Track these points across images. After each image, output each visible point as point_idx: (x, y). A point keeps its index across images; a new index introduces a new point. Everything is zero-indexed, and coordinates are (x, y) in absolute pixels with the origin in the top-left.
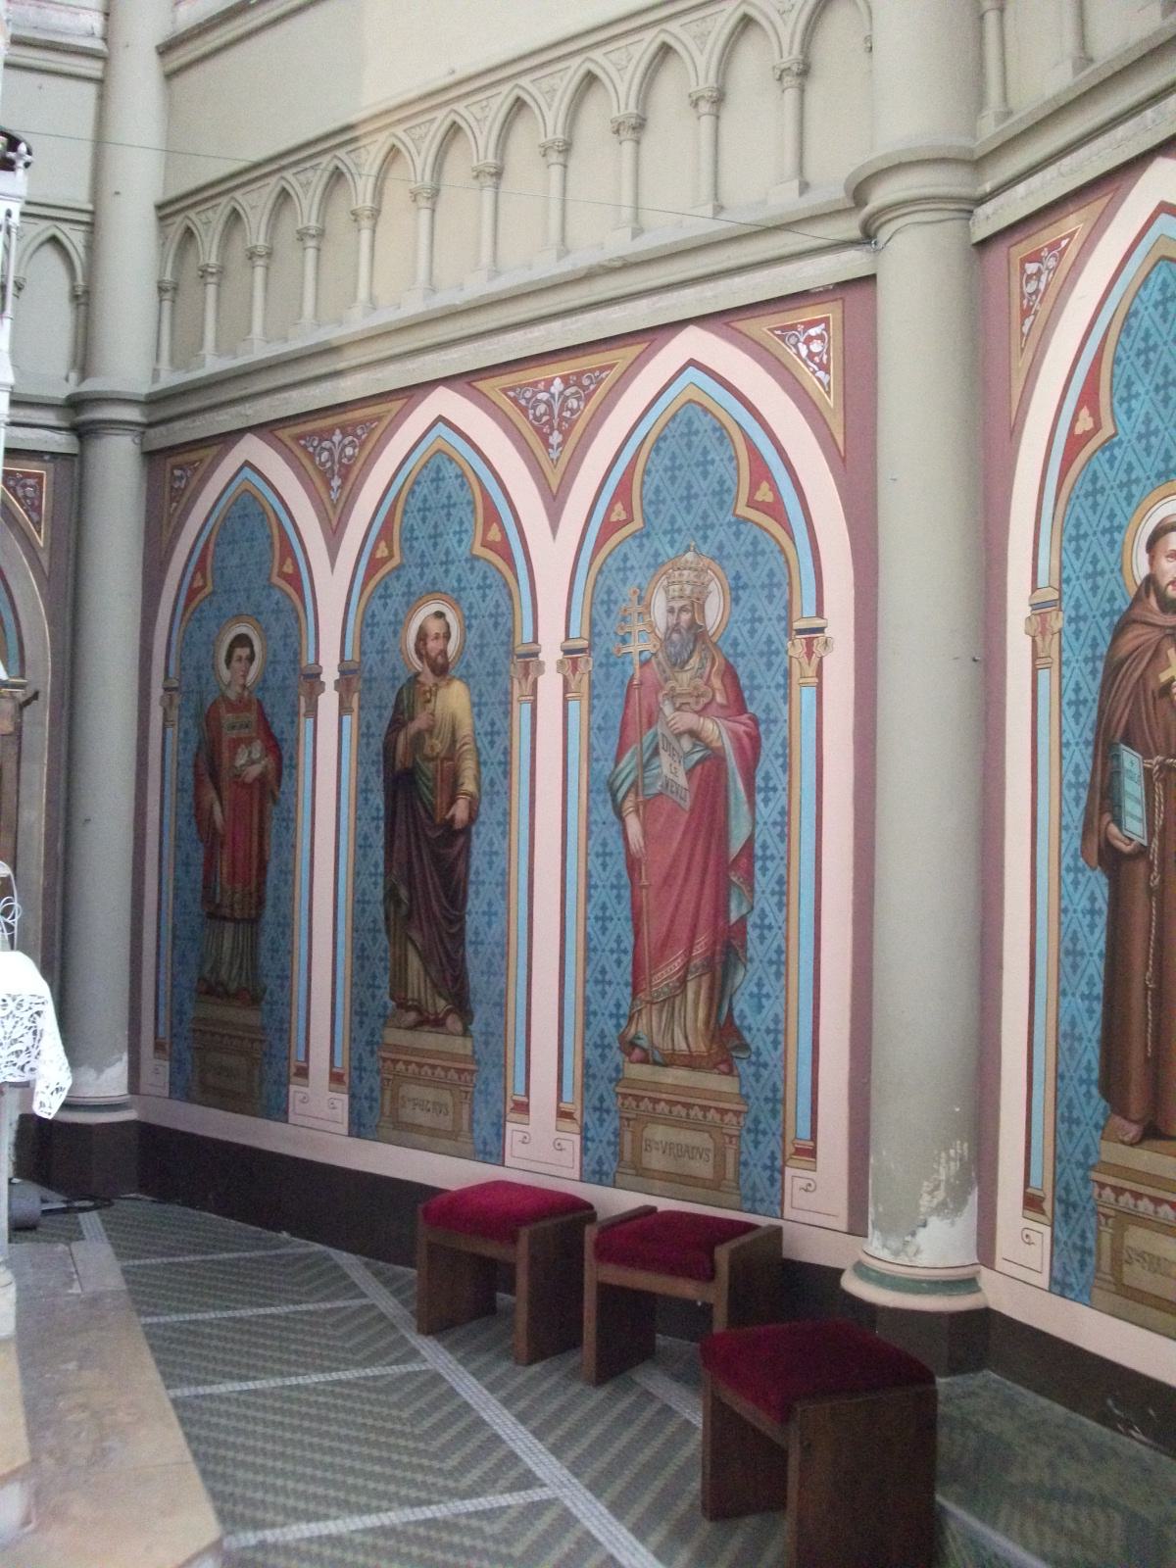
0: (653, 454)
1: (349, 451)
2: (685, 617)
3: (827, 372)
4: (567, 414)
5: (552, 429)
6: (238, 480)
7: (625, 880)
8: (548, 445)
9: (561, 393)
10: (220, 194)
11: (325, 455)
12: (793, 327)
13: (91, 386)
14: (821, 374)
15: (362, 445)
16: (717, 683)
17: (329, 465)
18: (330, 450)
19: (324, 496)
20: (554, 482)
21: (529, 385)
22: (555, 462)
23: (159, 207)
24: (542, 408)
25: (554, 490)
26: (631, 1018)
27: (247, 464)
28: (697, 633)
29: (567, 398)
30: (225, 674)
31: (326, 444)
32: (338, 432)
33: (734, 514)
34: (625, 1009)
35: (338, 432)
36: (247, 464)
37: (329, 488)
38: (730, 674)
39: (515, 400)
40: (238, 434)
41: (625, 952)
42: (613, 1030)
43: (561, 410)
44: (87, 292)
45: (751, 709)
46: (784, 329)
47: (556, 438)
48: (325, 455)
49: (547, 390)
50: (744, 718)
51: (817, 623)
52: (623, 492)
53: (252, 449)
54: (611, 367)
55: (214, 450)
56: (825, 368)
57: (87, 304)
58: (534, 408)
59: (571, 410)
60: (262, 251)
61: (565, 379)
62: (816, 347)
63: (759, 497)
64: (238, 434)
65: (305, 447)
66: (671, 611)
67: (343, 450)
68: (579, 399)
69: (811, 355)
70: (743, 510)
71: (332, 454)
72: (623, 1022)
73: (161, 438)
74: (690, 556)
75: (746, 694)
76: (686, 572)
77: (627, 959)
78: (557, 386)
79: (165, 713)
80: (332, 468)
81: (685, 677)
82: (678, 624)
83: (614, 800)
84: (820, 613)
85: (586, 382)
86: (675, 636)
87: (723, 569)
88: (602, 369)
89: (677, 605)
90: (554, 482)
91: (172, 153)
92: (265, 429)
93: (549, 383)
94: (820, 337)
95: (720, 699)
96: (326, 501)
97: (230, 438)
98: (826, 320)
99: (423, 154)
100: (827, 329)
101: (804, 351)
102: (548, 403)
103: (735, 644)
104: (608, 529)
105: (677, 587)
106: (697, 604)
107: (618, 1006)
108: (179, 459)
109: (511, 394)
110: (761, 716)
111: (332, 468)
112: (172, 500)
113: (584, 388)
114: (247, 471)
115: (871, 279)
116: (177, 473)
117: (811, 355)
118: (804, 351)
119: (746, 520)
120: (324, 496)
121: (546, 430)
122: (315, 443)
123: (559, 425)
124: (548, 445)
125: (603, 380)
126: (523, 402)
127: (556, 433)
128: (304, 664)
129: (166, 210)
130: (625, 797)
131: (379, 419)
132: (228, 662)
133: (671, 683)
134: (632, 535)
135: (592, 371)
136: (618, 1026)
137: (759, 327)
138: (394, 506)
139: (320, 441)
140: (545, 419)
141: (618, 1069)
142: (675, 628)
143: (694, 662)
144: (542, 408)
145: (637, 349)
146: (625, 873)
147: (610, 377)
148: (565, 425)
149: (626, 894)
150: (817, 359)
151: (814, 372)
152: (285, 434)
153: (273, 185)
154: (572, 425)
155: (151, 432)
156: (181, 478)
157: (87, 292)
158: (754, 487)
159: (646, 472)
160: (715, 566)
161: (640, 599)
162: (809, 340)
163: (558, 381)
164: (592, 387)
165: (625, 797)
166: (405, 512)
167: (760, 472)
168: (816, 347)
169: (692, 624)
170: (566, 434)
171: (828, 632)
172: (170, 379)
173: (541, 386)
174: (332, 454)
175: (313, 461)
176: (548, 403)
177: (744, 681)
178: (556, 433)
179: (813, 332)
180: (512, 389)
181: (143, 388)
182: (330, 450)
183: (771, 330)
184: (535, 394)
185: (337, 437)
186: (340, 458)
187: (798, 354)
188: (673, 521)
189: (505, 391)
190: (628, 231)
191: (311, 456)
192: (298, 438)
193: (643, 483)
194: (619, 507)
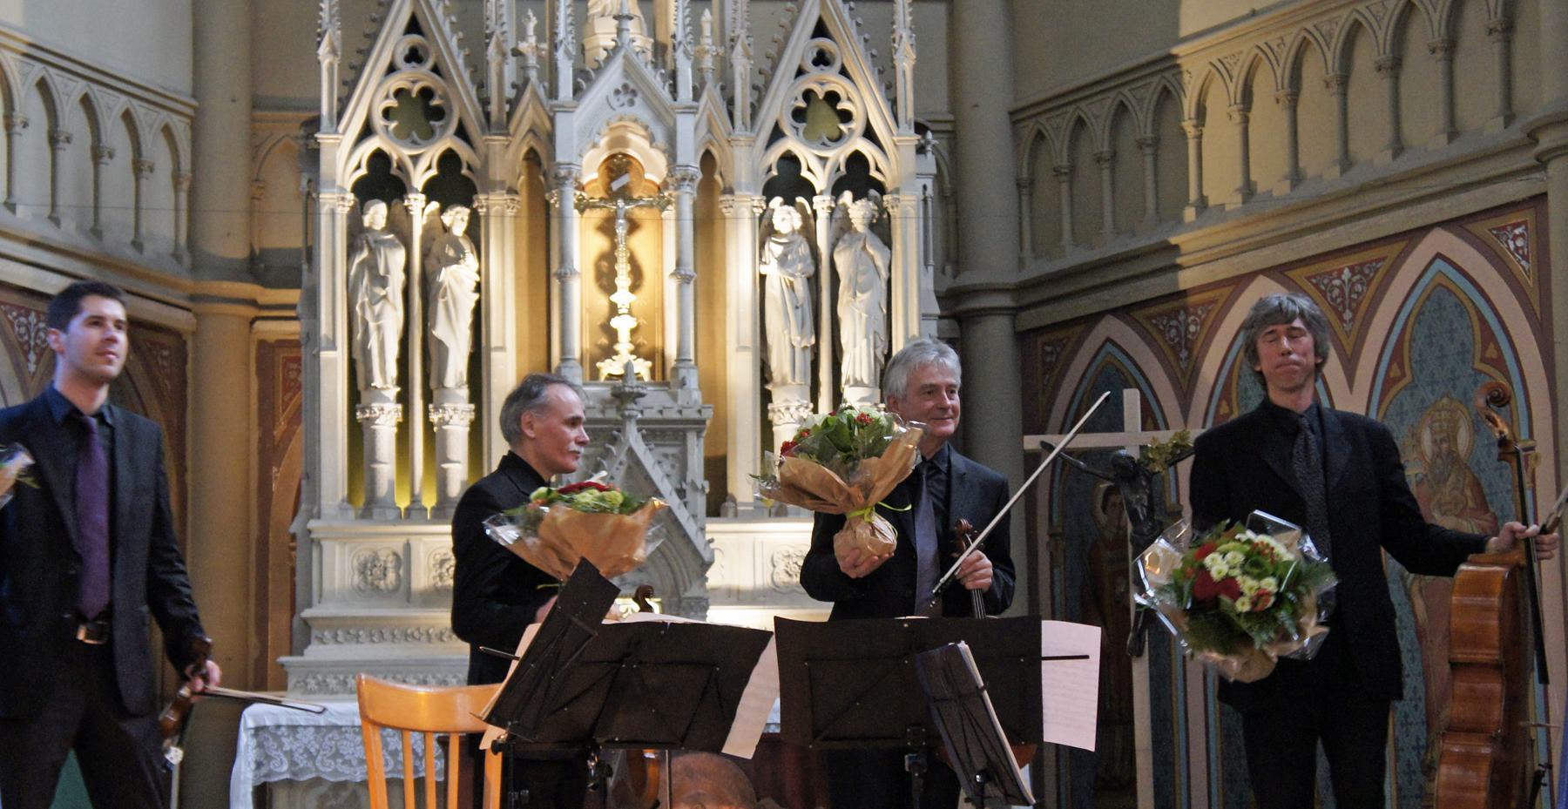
0: (1417, 325)
1: (1192, 328)
2: (1445, 446)
3: (1527, 261)
4: (1354, 296)
5: (1345, 308)
6: (1103, 353)
7: (1416, 645)
8: (1342, 320)
9: (1350, 280)
10: (1070, 103)
11: (1173, 331)
12: (1504, 228)
13: (968, 279)
14: (1523, 263)
15: (1202, 324)
16: (1468, 493)
17: (1177, 340)
18: (1177, 328)
19: (1174, 364)
20: (1349, 350)
21: (1327, 273)
22: (1348, 334)
23: (1012, 113)
24: (1336, 292)
25: (1349, 352)
26: (1427, 747)
27: (1109, 340)
28: (1453, 458)
29: (1353, 284)
30: (1103, 518)
31: (1174, 323)
32: (1182, 312)
33: (1473, 369)
34: (1423, 742)
35: (1182, 312)
36: (1109, 340)
37: (1178, 359)
38: (1477, 485)
39: (1316, 286)
40: (1099, 316)
41: (1420, 699)
42: (1416, 758)
43: (1350, 293)
44: (955, 193)
45: (1492, 509)
46: (1498, 229)
47: (1348, 315)
48: (1173, 331)
49: (1339, 277)
50: (1487, 516)
51: (1530, 443)
52: (1397, 357)
53: (1112, 327)
54: (1383, 259)
55: (1079, 329)
56: (1525, 258)
57: (956, 203)
58: (1331, 292)
59: (1357, 293)
60: (1107, 156)
61: (1352, 269)
62: (1520, 243)
63: (1488, 355)
64: (1099, 316)
65: (1156, 326)
66: (1434, 442)
67: (1187, 329)
68: (1362, 284)
69: (1517, 249)
70: (1478, 365)
71: (1178, 331)
72: (1422, 752)
73: (1030, 319)
74: (1445, 400)
75: (1488, 498)
76: (1443, 413)
77: (1422, 705)
78: (1346, 274)
79: (1052, 555)
80: (1179, 343)
81: (1447, 490)
82: (1440, 452)
83: (1405, 586)
84: (1531, 435)
85: (1367, 271)
86: (1439, 461)
87: (1468, 409)
88: (1378, 261)
89: (1438, 438)
90: (1349, 350)
91: (1017, 68)
92: (1124, 312)
93: (1341, 272)
94: (1522, 235)
95: (1471, 504)
96: (1177, 370)
97: (1093, 319)
98: (1525, 223)
99: (1234, 80)
100: (1526, 229)
101: (1512, 247)
102: (1341, 288)
103: (1478, 463)
104: (1389, 383)
105: (1437, 424)
106: (1452, 438)
107: (1418, 739)
108: (1045, 338)
109: (1314, 281)
110: (1498, 513)
111: (1179, 343)
112: (1045, 373)
113: (1366, 276)
114: (1109, 347)
115: (1544, 195)
116: (1048, 349)
117: (1517, 249)
118: (1512, 247)
119: (1480, 372)
120: (1174, 364)
121: (1340, 309)
122: (1165, 322)
123: (1350, 305)
124: (1342, 320)
125: (1378, 269)
126: (1323, 288)
127: (1347, 311)
128: (1168, 504)
129: (1016, 117)
130: (1412, 584)
131: (1213, 301)
132: (1104, 508)
133: (1439, 496)
134: (1405, 387)
135: (1371, 262)
136: (1419, 754)
137: (1481, 228)
138: (1231, 371)
139: (1169, 321)
140: (1339, 300)
141: (1421, 787)
142: (1437, 455)
143: (1452, 479)
144: (1336, 292)
145: (1402, 245)
146: (1416, 640)
147: (1383, 267)
148: (1354, 305)
149: (1417, 655)
150: (1521, 252)
151: (1519, 261)
152: (1139, 314)
153: (1108, 103)
154: (1359, 304)
155: (1023, 314)
156: (1051, 353)
157: (955, 193)
158: (1484, 349)
159: (1412, 340)
160: (1461, 407)
161: (1413, 435)
162: (1515, 238)
163: (1346, 271)
164: (1372, 275)
165: (1412, 584)
166: (1239, 377)
167: (1488, 336)
168: (1520, 243)
169: (1450, 452)
170: (1355, 312)
171: (1537, 450)
172: (1036, 269)
173: (1335, 274)
174: (1178, 331)
175: (1164, 337)
176: (1341, 288)
177: (1486, 490)
178: (1347, 311)
179: (1517, 231)
180: (1315, 277)
181: (1013, 279)
182: (1177, 328)
183: (1490, 230)
184: (1331, 281)
185: (1182, 317)
186: (1186, 335)
187: (1509, 249)
188: (1432, 375)
189: (1309, 278)
190: (1389, 153)
191: (1162, 333)
192: (1149, 318)
193: (1410, 347)
194: (1395, 366)
